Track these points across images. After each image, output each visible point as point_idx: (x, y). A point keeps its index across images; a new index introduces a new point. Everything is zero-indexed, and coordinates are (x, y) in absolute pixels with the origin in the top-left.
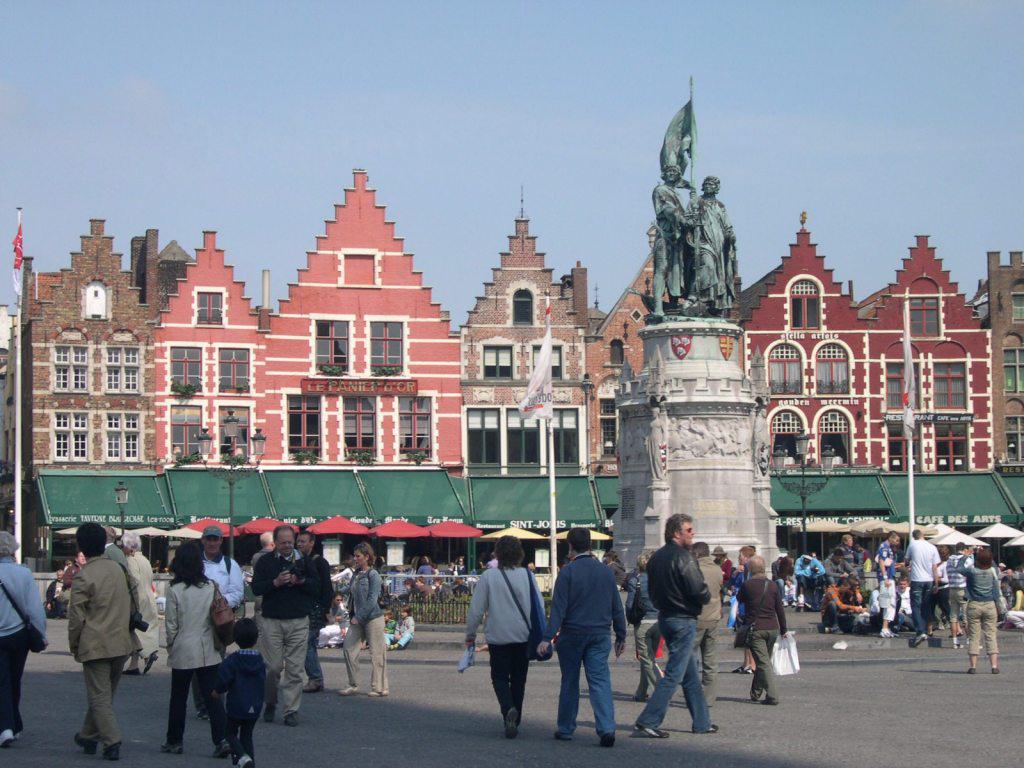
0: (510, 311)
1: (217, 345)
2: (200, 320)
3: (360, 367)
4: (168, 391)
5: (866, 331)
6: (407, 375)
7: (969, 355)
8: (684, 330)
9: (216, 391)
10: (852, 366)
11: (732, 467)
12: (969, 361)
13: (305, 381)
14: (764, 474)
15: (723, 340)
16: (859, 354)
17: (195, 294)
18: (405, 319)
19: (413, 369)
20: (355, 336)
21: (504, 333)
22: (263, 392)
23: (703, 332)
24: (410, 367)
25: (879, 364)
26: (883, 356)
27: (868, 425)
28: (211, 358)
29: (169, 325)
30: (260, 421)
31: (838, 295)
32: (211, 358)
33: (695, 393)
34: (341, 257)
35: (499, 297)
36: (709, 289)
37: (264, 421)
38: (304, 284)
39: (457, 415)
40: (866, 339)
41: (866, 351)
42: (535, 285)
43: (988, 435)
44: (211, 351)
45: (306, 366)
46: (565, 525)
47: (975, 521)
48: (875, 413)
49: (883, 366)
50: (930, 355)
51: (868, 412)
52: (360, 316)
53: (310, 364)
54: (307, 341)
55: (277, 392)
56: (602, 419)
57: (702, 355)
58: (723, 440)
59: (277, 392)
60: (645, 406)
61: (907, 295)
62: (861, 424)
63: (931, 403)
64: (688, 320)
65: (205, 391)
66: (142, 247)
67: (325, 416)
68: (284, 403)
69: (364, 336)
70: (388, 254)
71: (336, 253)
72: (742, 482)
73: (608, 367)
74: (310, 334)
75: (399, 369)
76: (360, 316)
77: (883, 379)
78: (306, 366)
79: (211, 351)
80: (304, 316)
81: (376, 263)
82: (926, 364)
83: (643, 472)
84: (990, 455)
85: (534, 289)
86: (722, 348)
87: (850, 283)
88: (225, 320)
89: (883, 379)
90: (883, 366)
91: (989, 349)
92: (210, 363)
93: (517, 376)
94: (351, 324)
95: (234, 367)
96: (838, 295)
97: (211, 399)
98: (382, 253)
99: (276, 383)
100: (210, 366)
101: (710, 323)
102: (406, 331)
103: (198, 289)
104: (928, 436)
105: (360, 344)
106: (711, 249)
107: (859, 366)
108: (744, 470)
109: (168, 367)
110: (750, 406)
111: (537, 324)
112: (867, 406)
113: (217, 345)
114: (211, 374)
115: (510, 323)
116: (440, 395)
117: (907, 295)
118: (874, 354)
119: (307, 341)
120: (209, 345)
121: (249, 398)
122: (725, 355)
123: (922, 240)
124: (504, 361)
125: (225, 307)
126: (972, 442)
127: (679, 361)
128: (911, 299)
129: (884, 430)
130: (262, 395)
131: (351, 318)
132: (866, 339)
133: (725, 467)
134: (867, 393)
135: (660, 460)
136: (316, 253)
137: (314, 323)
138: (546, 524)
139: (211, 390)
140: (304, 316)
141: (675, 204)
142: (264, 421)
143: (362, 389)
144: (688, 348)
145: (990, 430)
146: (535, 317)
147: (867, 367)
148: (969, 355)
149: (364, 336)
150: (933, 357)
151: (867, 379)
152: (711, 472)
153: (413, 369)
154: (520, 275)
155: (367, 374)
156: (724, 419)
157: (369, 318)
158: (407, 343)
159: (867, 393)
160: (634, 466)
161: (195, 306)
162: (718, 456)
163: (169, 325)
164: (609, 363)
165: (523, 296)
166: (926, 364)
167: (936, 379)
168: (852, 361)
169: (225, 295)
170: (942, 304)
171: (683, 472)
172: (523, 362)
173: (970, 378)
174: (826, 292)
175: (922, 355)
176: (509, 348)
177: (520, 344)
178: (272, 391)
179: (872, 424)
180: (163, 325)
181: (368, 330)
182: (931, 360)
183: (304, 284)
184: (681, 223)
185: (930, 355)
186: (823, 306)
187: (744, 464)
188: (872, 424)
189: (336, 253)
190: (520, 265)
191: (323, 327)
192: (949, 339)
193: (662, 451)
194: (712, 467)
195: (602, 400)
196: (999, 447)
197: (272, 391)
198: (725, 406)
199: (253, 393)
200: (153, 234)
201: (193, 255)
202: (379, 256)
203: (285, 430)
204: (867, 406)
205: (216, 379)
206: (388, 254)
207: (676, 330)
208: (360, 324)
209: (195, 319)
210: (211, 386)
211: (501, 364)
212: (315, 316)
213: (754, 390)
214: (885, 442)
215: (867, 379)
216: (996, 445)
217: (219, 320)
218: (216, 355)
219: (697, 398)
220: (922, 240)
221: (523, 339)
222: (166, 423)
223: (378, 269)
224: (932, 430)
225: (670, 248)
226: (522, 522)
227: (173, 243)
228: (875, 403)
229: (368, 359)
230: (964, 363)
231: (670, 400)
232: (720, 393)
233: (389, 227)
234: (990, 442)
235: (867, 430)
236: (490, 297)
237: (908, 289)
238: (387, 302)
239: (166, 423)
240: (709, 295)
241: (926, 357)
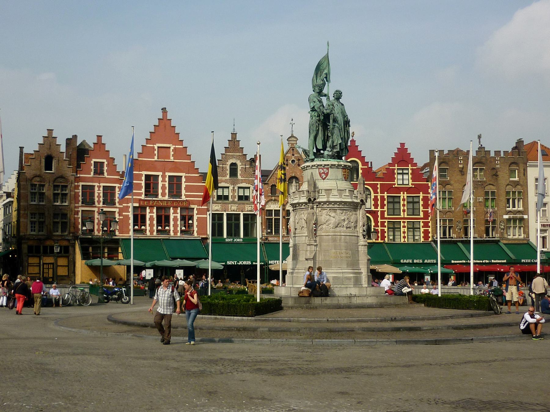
0: (228, 172)
1: (102, 185)
2: (95, 173)
3: (163, 195)
4: (80, 203)
5: (379, 183)
6: (184, 198)
7: (421, 193)
8: (325, 165)
9: (101, 205)
10: (373, 197)
11: (348, 234)
12: (421, 195)
13: (140, 200)
14: (364, 238)
16: (375, 192)
17: (92, 162)
18: (183, 175)
19: (187, 196)
20: (162, 181)
21: (226, 181)
22: (122, 205)
23: (333, 166)
24: (185, 195)
25: (384, 196)
26: (386, 193)
27: (380, 222)
28: (99, 190)
29: (81, 175)
30: (120, 217)
31: (366, 167)
32: (99, 190)
33: (331, 196)
34: (156, 148)
35: (224, 166)
36: (337, 145)
37: (122, 217)
38: (140, 159)
39: (206, 216)
40: (379, 186)
41: (379, 190)
42: (239, 161)
43: (429, 227)
44: (99, 187)
45: (140, 194)
46: (250, 263)
47: (425, 262)
48: (383, 217)
49: (386, 197)
50: (405, 193)
51: (379, 216)
52: (164, 173)
53: (142, 193)
54: (141, 183)
55: (128, 205)
56: (267, 218)
57: (334, 178)
59: (128, 205)
60: (306, 203)
61: (396, 167)
62: (376, 222)
63: (406, 213)
64: (327, 160)
65: (96, 204)
66: (70, 142)
67: (148, 216)
68: (131, 210)
69: (166, 182)
70: (176, 146)
71: (154, 146)
73: (270, 196)
74: (142, 181)
75: (180, 196)
76: (164, 173)
77: (386, 202)
78: (140, 194)
79: (99, 187)
80: (140, 173)
81: (171, 150)
82: (404, 196)
83: (304, 236)
84: (430, 235)
85: (239, 163)
86: (344, 175)
87: (371, 163)
88: (106, 174)
89: (386, 202)
90: (386, 197)
91: (430, 191)
92: (98, 192)
93: (230, 199)
94: (160, 177)
95: (109, 193)
96: (366, 167)
97: (99, 208)
98: (174, 146)
99: (128, 201)
100: (99, 193)
101: (338, 162)
102: (184, 180)
103: (94, 160)
104: (404, 227)
105: (163, 184)
106: (338, 126)
107: (376, 197)
108: (355, 236)
109: (80, 194)
110: (357, 203)
111: (239, 177)
112: (379, 214)
113: (102, 185)
114: (99, 197)
115: (228, 177)
116: (198, 207)
117: (396, 167)
118: (382, 192)
119: (141, 183)
120: (99, 185)
121: (116, 207)
122: (345, 178)
123: (402, 145)
124: (226, 194)
125: (105, 168)
126: (422, 230)
127: (323, 181)
128: (397, 169)
129: (386, 224)
130: (122, 206)
131: (160, 174)
132: (379, 186)
134: (379, 209)
136: (146, 146)
137: (144, 175)
138: (242, 263)
139: (99, 204)
140: (140, 173)
141: (320, 102)
142: (122, 217)
143: (165, 204)
144: (327, 174)
145: (430, 224)
146: (239, 175)
147: (379, 197)
148: (421, 193)
149: (166, 182)
150: (407, 194)
151: (379, 203)
152: (339, 236)
153: (187, 196)
154: (233, 157)
155: (166, 198)
157: (168, 174)
158: (184, 185)
159: (379, 209)
160: (299, 233)
161: (92, 167)
162: (342, 228)
163: (81, 175)
164: (270, 195)
165: (234, 165)
166: (404, 196)
167: (408, 202)
168: (373, 195)
169: (106, 163)
170: (410, 171)
171: (325, 237)
172: (234, 194)
173: (421, 203)
174: (362, 166)
175: (402, 193)
176: (228, 187)
177: (233, 186)
178: (126, 205)
179: (381, 222)
180: (78, 176)
181: (167, 179)
182: (406, 195)
183: (140, 159)
184: (323, 113)
185: (405, 193)
186: (360, 171)
188: (381, 222)
189: (154, 146)
190: (233, 153)
191: (148, 177)
192: (413, 186)
193: (314, 226)
195: (267, 210)
196: (434, 232)
197: (126, 205)
198: (345, 203)
199: (117, 205)
200: (75, 137)
201: (92, 146)
202: (172, 148)
203: (131, 221)
204: (379, 214)
205: (101, 199)
206: (176, 146)
207: (321, 165)
208: (164, 177)
209: (92, 173)
210: (99, 202)
211: (224, 194)
212: (144, 173)
213: (359, 196)
214: (386, 229)
215: (379, 203)
216: (432, 231)
217: (103, 174)
218: (101, 189)
219: (331, 200)
220: (402, 145)
221: (234, 184)
222: (79, 218)
223: (172, 153)
224: (406, 224)
225: (317, 124)
226: (232, 262)
227: (84, 141)
228: (383, 213)
229: (167, 191)
230: (419, 196)
231: (318, 200)
232: (343, 197)
233: (178, 135)
234: (430, 230)
235: (379, 224)
236: (220, 166)
237: (396, 165)
238: (176, 167)
239: (79, 218)
240: (337, 149)
241: (404, 194)
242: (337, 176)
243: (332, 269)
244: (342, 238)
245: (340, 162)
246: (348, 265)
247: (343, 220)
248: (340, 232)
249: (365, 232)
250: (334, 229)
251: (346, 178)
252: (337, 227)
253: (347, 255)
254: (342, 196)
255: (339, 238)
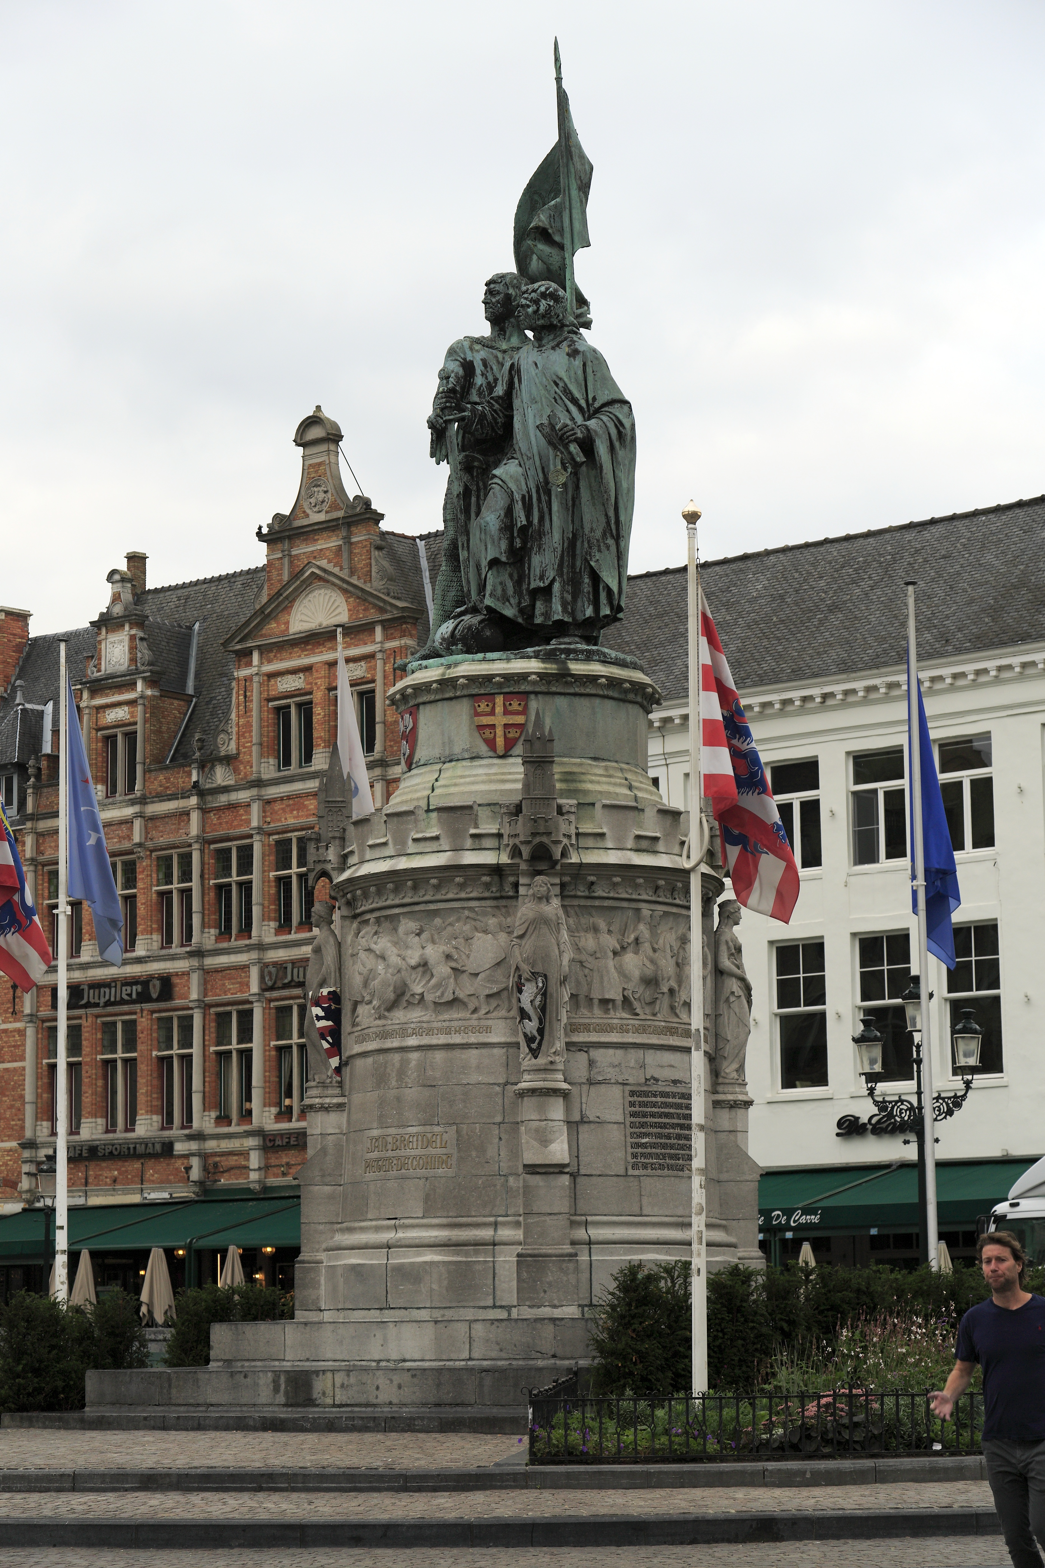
11: (442, 1040)
15: (483, 707)
57: (436, 752)
58: (424, 966)
72: (475, 1078)
86: (481, 727)
110: (497, 870)
122: (491, 744)
133: (426, 1040)
135: (315, 1035)
152: (396, 1057)
156: (436, 913)
162: (415, 1015)
187: (488, 1030)
193: (317, 1011)
194: (395, 1043)
198: (418, 877)
232: (412, 848)
242: (451, 741)
243: (363, 1229)
244: (408, 1061)
245: (456, 664)
246: (430, 1206)
247: (414, 968)
248: (403, 1033)
249: (530, 1020)
250: (385, 1018)
251: (500, 742)
252: (392, 1006)
253: (431, 1151)
254: (404, 844)
255: (397, 1065)
